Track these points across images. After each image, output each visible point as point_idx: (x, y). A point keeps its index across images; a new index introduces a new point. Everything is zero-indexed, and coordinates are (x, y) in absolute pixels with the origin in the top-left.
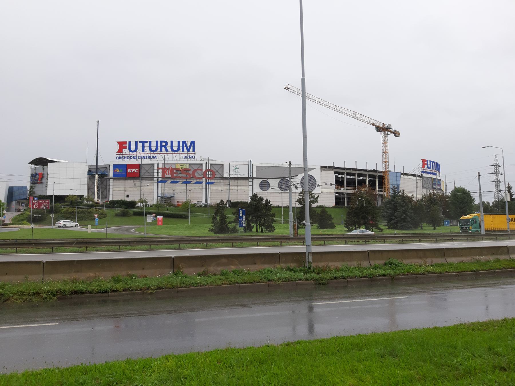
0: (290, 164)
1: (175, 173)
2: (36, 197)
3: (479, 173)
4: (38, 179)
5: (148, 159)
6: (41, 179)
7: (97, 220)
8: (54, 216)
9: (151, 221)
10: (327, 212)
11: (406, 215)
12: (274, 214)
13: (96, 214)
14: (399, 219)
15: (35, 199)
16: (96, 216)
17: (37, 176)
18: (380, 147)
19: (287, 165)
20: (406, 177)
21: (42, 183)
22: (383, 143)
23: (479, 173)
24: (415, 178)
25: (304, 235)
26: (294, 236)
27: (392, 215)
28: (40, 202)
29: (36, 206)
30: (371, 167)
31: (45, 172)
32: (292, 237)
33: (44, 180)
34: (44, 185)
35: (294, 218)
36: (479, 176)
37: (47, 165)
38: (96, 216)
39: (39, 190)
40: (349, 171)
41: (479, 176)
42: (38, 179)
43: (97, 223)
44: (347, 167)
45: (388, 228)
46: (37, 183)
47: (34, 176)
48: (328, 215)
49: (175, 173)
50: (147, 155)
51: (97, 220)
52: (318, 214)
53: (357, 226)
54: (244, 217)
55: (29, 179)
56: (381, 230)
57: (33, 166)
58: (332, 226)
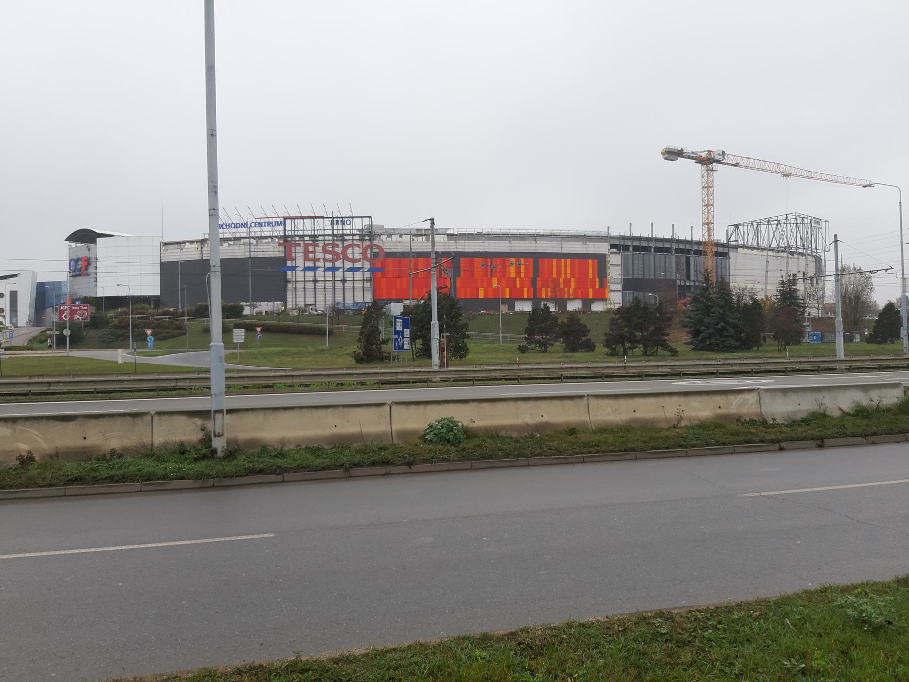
0: (433, 223)
1: (311, 252)
2: (78, 300)
3: (836, 236)
4: (82, 268)
5: (270, 228)
6: (86, 268)
7: (150, 339)
8: (69, 333)
9: (242, 341)
10: (579, 319)
11: (727, 323)
12: (466, 324)
13: (148, 328)
14: (712, 331)
15: (77, 303)
16: (149, 332)
17: (80, 263)
18: (697, 194)
19: (427, 225)
20: (746, 251)
21: (87, 275)
22: (703, 188)
23: (836, 236)
24: (765, 253)
25: (208, 371)
26: (440, 366)
27: (700, 322)
28: (73, 308)
29: (66, 317)
30: (683, 234)
31: (92, 256)
32: (436, 368)
33: (91, 269)
34: (92, 279)
35: (441, 331)
36: (836, 241)
37: (95, 242)
38: (149, 332)
39: (83, 288)
40: (636, 243)
41: (836, 241)
42: (82, 268)
43: (150, 344)
44: (636, 234)
45: (693, 349)
46: (79, 275)
47: (74, 261)
48: (580, 325)
49: (311, 252)
50: (267, 220)
51: (150, 339)
52: (563, 323)
53: (628, 345)
54: (407, 332)
55: (65, 267)
56: (674, 353)
57: (73, 245)
58: (589, 347)
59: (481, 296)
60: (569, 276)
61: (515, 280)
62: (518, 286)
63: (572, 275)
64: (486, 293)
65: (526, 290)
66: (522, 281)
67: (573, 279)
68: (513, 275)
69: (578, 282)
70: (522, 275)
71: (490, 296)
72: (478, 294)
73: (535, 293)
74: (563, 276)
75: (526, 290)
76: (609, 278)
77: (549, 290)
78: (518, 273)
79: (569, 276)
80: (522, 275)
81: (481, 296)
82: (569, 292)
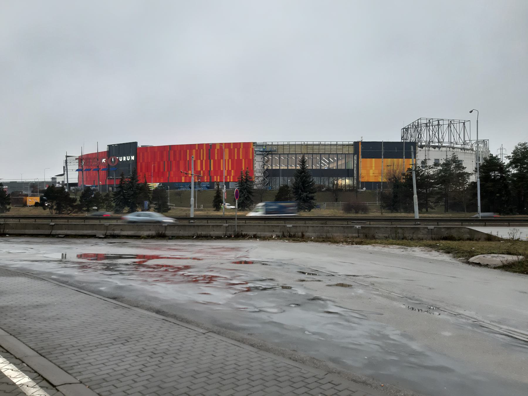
59: (183, 181)
60: (230, 169)
61: (200, 172)
62: (202, 175)
63: (232, 169)
64: (185, 179)
65: (205, 177)
66: (204, 172)
67: (232, 171)
68: (199, 169)
69: (236, 172)
70: (204, 169)
71: (188, 181)
72: (181, 180)
73: (210, 179)
74: (227, 169)
75: (205, 177)
76: (255, 169)
77: (219, 177)
78: (202, 168)
79: (230, 169)
80: (204, 169)
81: (183, 181)
82: (230, 179)
